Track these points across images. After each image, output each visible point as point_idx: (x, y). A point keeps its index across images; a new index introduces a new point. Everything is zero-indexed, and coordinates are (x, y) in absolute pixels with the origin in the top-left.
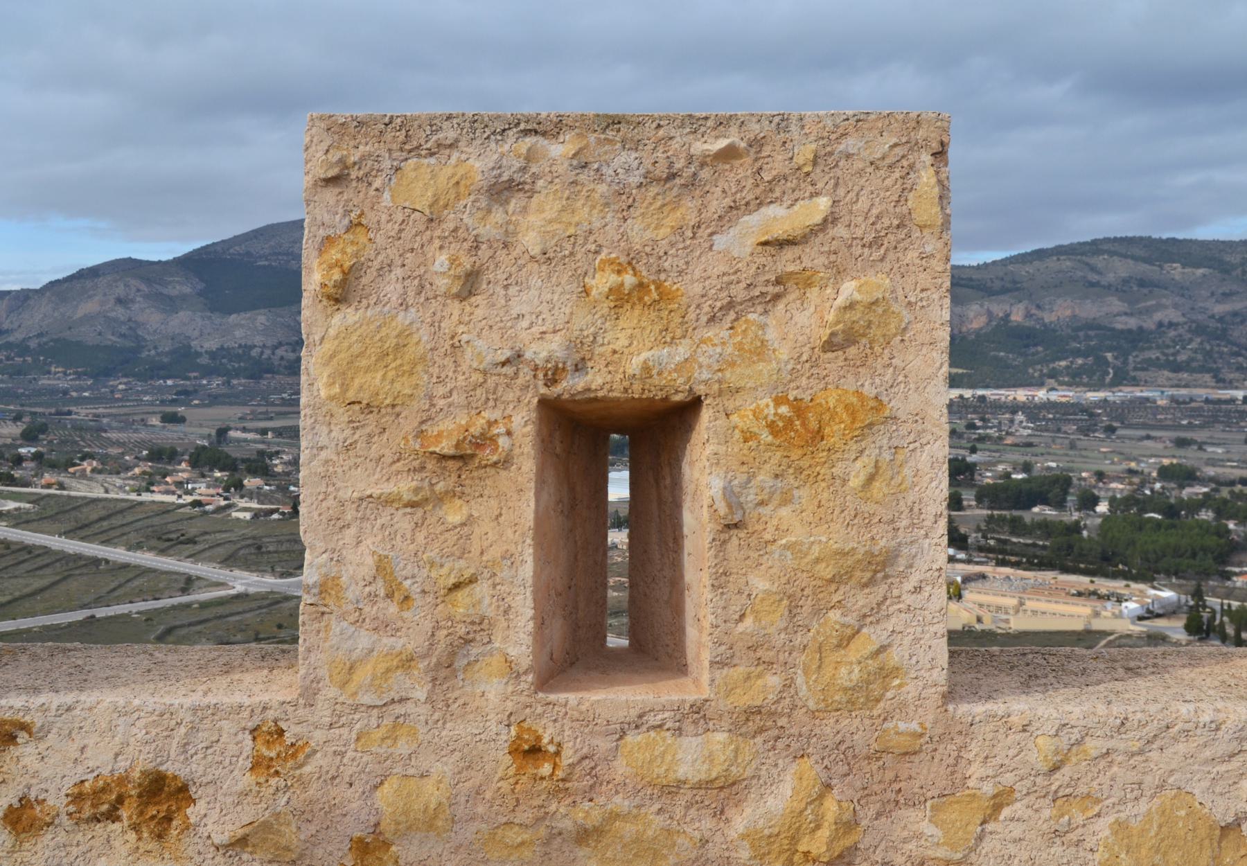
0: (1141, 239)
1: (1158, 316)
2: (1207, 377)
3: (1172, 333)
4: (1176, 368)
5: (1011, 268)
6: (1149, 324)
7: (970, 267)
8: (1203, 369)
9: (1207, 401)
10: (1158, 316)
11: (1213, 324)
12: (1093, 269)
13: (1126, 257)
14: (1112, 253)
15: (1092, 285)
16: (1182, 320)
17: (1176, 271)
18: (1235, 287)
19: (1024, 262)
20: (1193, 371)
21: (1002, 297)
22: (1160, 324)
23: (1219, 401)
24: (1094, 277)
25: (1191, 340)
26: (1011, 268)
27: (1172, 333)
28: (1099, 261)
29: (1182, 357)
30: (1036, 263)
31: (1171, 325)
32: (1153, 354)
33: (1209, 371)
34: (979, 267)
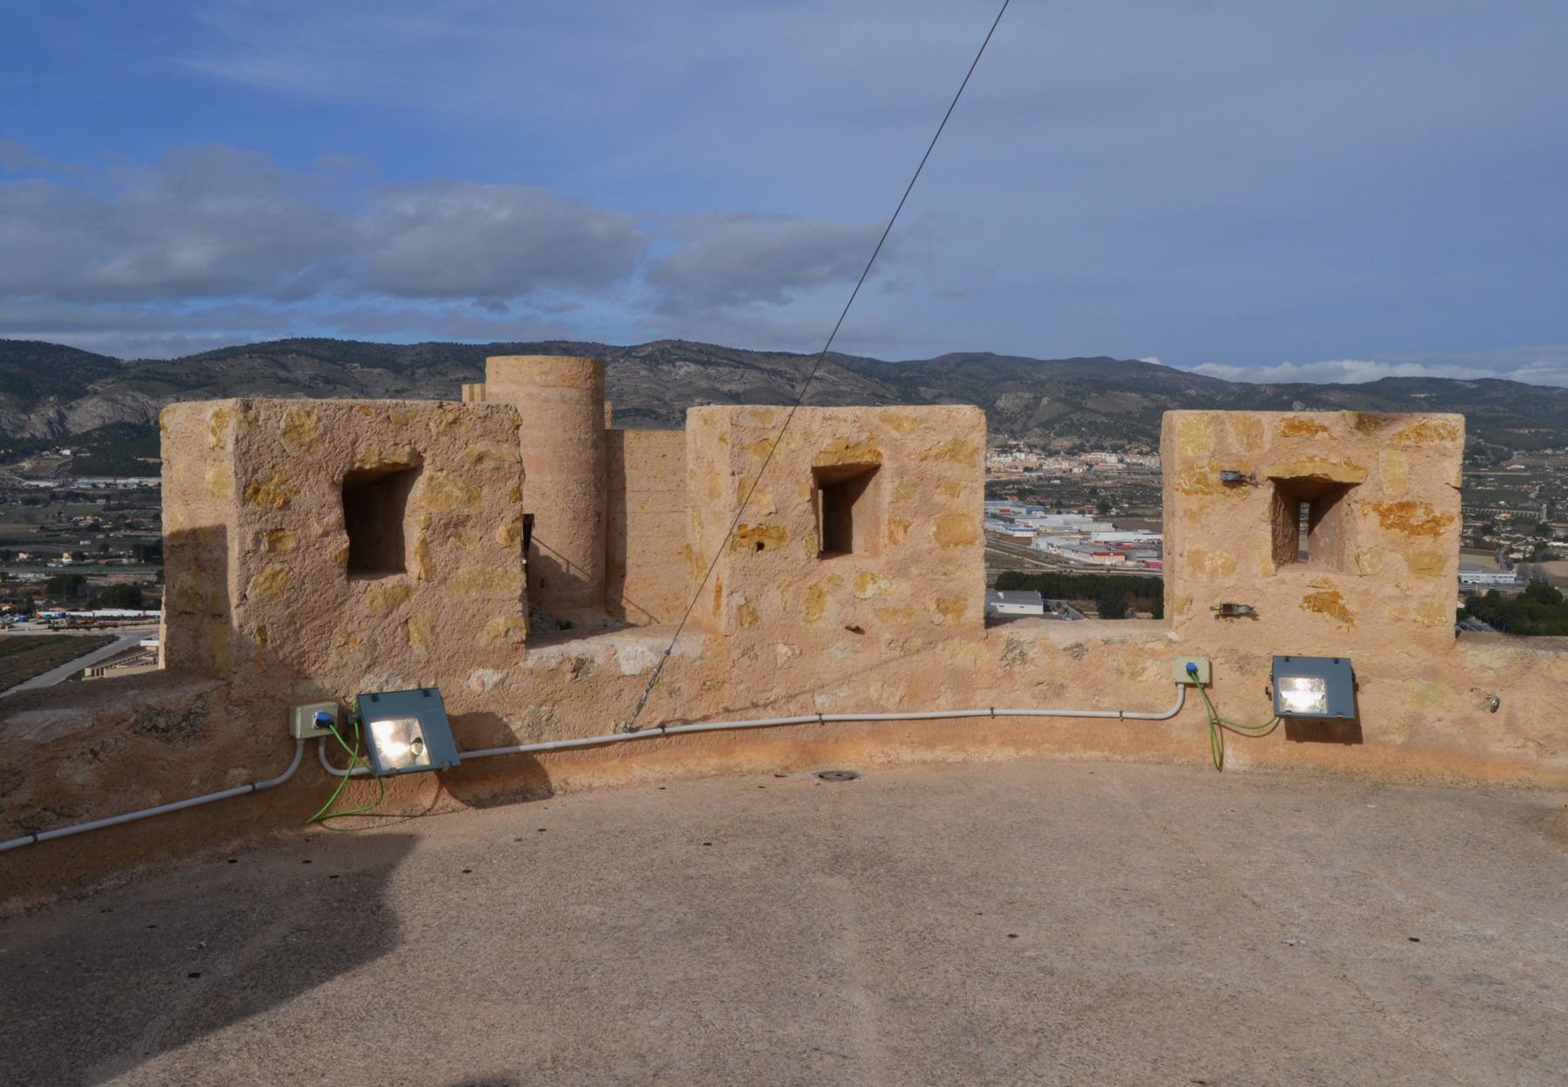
0: (326, 340)
5: (205, 364)
7: (164, 362)
12: (284, 367)
13: (312, 356)
14: (299, 353)
15: (287, 380)
17: (356, 369)
18: (405, 385)
19: (218, 359)
21: (197, 391)
24: (283, 374)
26: (205, 364)
28: (288, 359)
30: (230, 360)
34: (173, 362)
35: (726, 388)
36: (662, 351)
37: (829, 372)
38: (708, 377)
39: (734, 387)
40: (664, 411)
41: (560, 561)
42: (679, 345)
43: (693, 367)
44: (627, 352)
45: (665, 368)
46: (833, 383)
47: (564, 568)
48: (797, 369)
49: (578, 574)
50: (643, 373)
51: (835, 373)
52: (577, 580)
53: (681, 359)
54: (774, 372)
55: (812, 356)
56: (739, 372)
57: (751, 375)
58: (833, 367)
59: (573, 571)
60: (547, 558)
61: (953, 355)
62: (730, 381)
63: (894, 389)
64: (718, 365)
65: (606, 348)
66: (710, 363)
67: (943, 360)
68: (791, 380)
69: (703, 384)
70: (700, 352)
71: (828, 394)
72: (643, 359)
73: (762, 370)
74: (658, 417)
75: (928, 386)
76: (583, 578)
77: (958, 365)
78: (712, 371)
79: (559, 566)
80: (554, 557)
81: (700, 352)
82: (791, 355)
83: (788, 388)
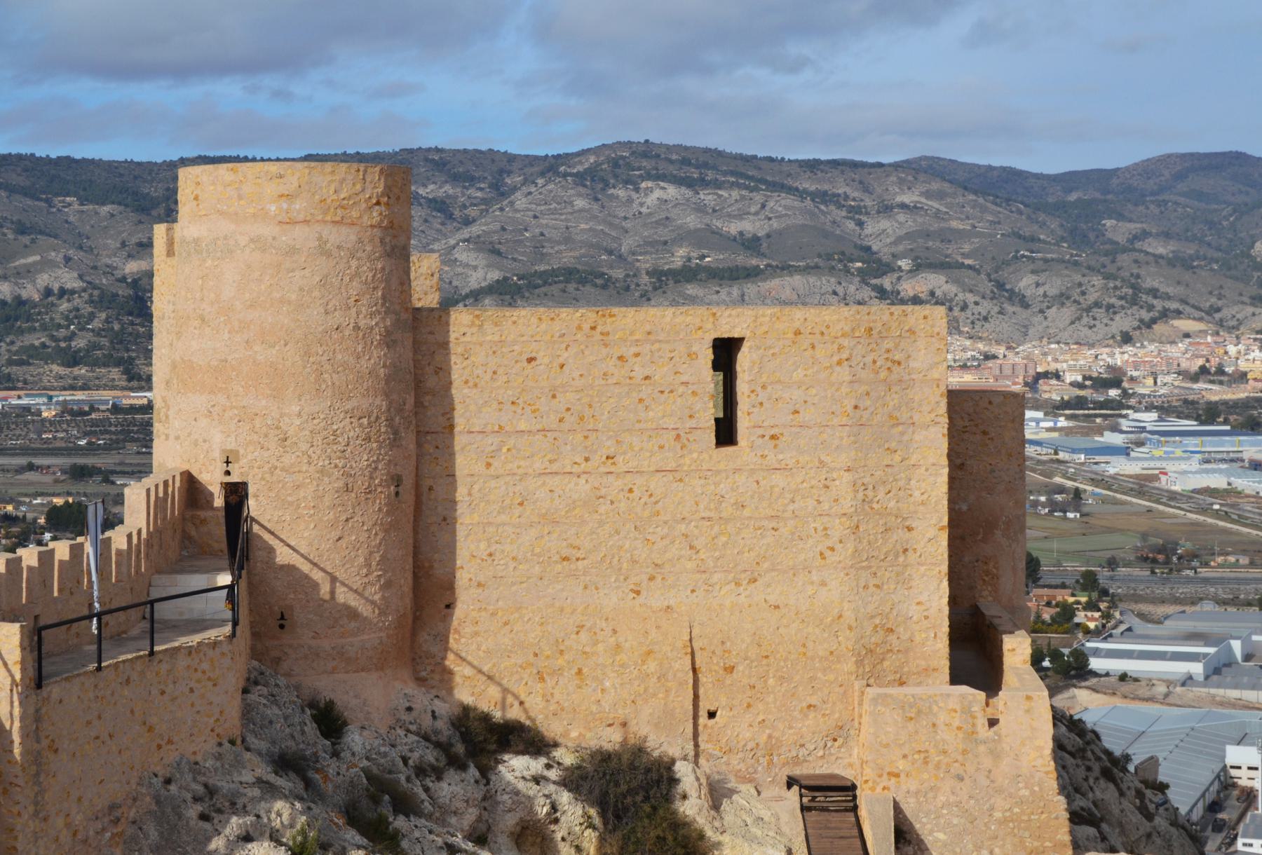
1: (43, 280)
2: (115, 373)
3: (64, 306)
4: (73, 359)
6: (31, 292)
8: (108, 362)
9: (116, 409)
10: (43, 280)
11: (123, 291)
16: (77, 284)
20: (95, 364)
22: (48, 292)
23: (133, 409)
25: (92, 316)
27: (64, 306)
29: (80, 343)
31: (63, 292)
32: (37, 339)
33: (118, 363)
35: (733, 228)
36: (615, 164)
37: (928, 194)
38: (700, 209)
39: (748, 226)
40: (618, 273)
41: (317, 575)
42: (647, 150)
43: (672, 191)
44: (551, 166)
45: (621, 193)
46: (937, 215)
47: (325, 590)
48: (867, 190)
49: (353, 601)
50: (580, 203)
51: (940, 196)
52: (353, 614)
53: (648, 177)
54: (823, 197)
55: (896, 166)
56: (758, 197)
57: (780, 203)
58: (935, 186)
59: (343, 596)
60: (290, 569)
61: (1166, 159)
62: (740, 216)
63: (1054, 224)
64: (718, 185)
65: (511, 158)
66: (703, 183)
67: (1148, 168)
68: (856, 212)
69: (692, 221)
70: (685, 162)
71: (929, 235)
72: (580, 178)
73: (801, 194)
74: (608, 283)
75: (1120, 217)
76: (365, 610)
77: (1180, 177)
78: (707, 197)
79: (316, 585)
80: (305, 567)
81: (685, 162)
82: (855, 165)
83: (851, 225)
